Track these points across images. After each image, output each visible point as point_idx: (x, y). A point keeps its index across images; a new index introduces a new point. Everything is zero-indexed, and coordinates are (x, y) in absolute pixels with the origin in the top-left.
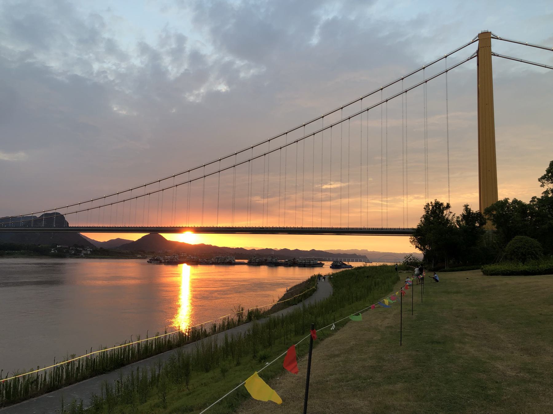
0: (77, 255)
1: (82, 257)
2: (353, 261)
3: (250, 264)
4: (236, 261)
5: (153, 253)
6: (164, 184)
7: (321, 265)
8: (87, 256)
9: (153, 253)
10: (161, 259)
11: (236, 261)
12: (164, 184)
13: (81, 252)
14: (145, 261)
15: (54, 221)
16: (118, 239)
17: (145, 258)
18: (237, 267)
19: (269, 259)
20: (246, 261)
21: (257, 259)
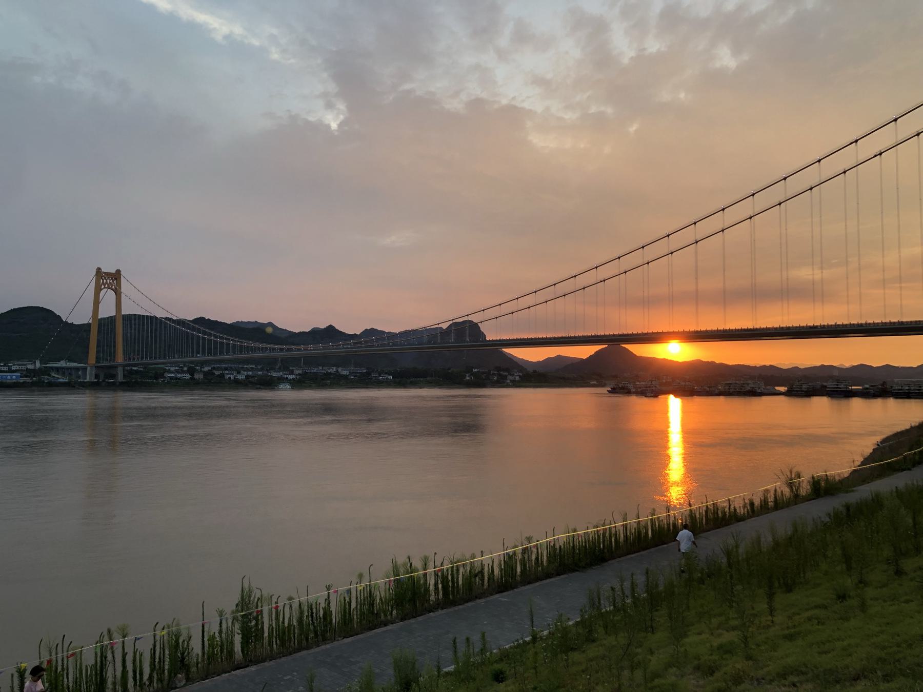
0: (500, 383)
1: (508, 386)
3: (789, 394)
5: (615, 377)
6: (626, 263)
8: (516, 385)
9: (615, 377)
10: (630, 386)
12: (626, 263)
13: (505, 377)
14: (604, 390)
15: (465, 332)
16: (559, 357)
17: (603, 386)
18: (764, 398)
20: (783, 389)
21: (805, 385)
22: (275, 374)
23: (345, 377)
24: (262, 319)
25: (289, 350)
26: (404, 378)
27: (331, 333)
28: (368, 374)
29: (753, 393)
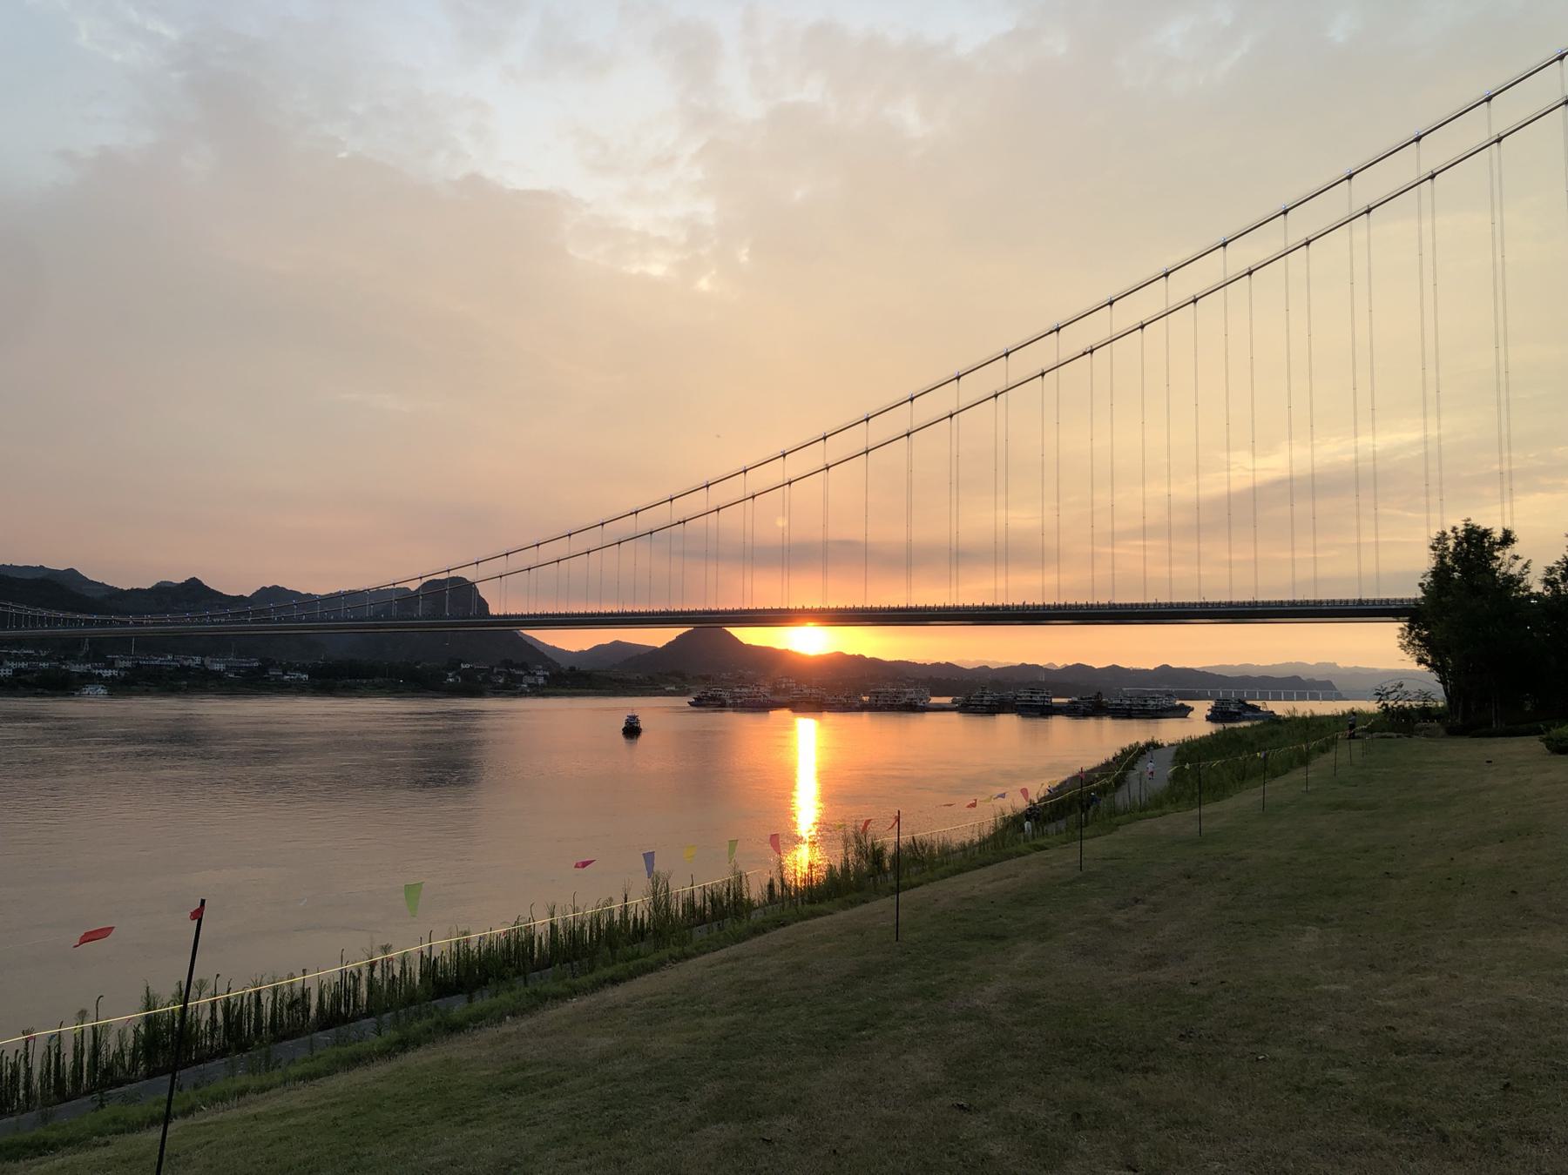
0: (511, 689)
2: (1277, 698)
4: (934, 700)
7: (1183, 712)
8: (538, 691)
9: (706, 679)
10: (725, 695)
11: (934, 700)
13: (521, 677)
14: (683, 702)
15: (452, 598)
16: (617, 645)
18: (929, 716)
19: (1024, 695)
22: (77, 668)
23: (218, 675)
24: (56, 560)
25: (103, 623)
26: (333, 678)
27: (193, 593)
28: (263, 669)
29: (913, 708)
